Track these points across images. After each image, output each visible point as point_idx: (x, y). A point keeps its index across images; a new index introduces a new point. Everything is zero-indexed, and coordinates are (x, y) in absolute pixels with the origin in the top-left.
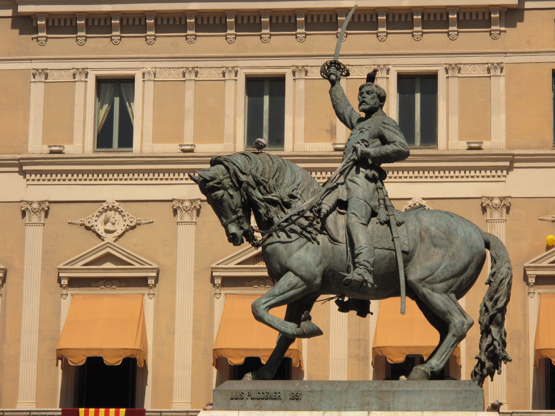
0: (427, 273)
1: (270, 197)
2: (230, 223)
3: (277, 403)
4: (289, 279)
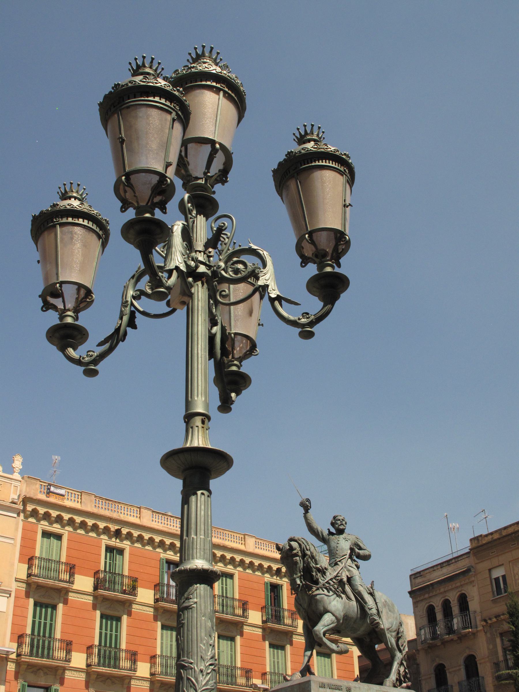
1: (318, 566)
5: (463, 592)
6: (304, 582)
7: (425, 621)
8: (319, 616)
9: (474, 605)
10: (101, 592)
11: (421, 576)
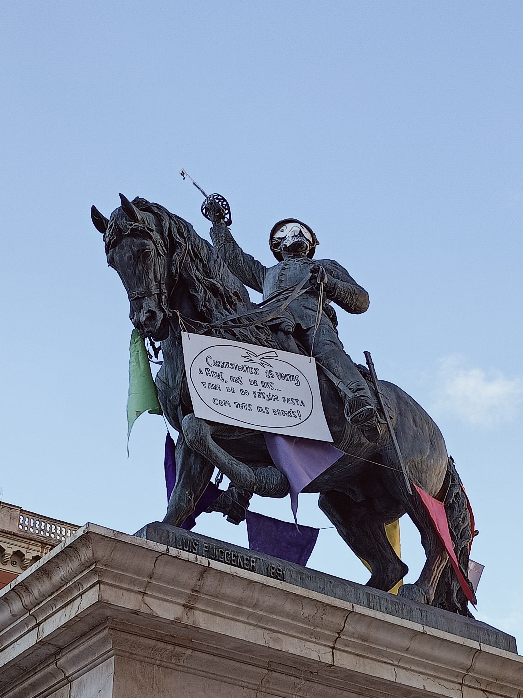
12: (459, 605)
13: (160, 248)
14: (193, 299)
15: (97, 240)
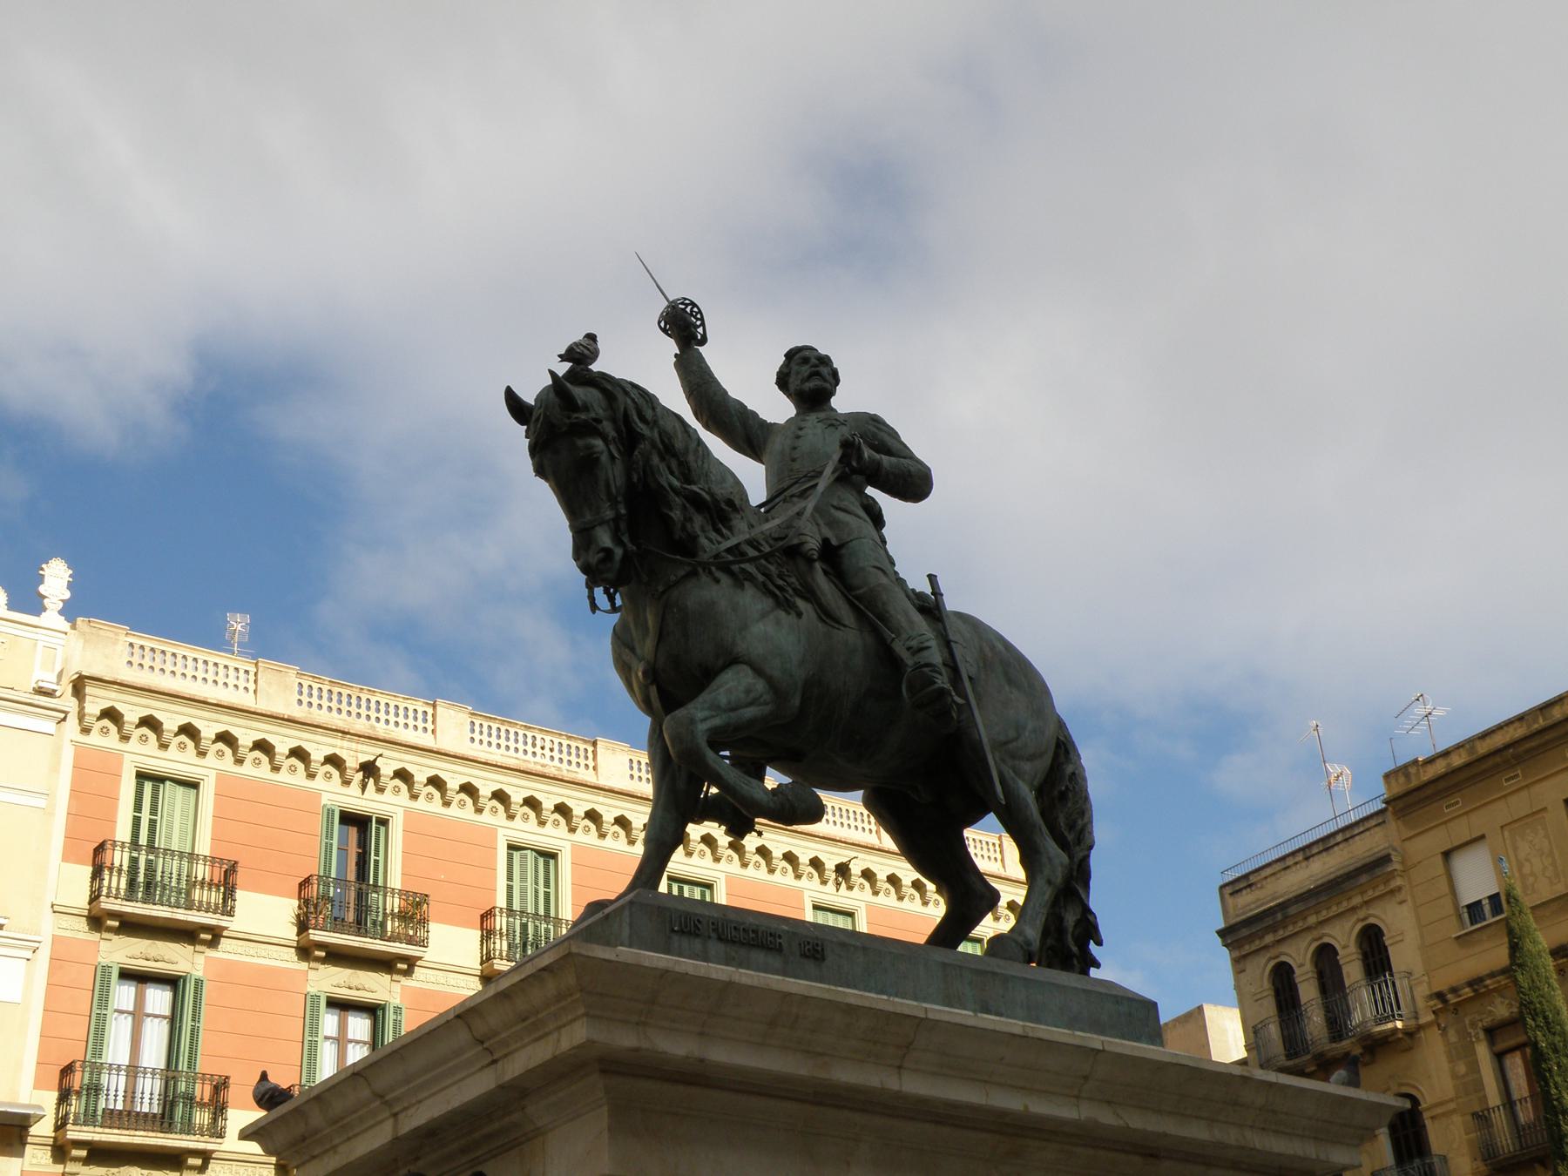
0: (1012, 734)
2: (600, 524)
3: (775, 961)
4: (733, 685)
5: (1372, 920)
6: (631, 547)
7: (1269, 1008)
8: (704, 677)
9: (1403, 955)
10: (316, 935)
11: (1250, 886)
12: (1075, 949)
13: (612, 447)
14: (667, 522)
15: (517, 437)
